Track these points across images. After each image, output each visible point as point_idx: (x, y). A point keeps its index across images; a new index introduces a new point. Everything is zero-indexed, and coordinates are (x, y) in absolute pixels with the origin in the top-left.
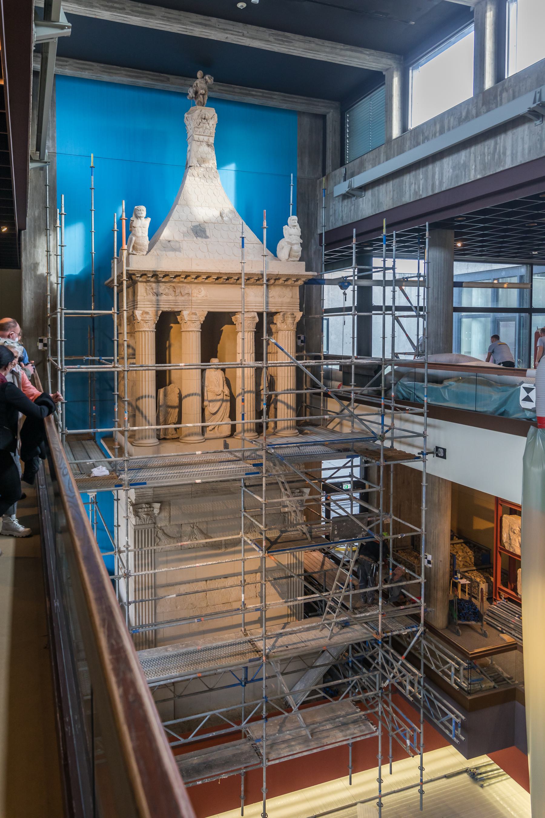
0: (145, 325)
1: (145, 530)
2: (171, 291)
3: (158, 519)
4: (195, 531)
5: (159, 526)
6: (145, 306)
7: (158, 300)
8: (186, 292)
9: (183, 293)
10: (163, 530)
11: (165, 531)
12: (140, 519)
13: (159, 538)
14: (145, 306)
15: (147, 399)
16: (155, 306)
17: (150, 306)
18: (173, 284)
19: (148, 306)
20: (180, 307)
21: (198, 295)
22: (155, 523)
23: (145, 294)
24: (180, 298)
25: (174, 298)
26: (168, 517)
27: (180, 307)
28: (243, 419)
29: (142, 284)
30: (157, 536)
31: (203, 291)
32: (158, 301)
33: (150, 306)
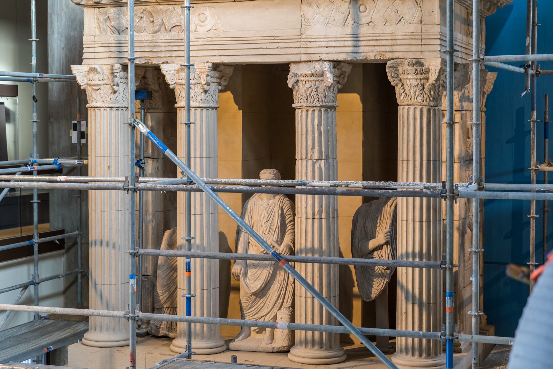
0: (94, 95)
2: (145, 23)
6: (97, 55)
7: (119, 42)
8: (174, 22)
9: (167, 24)
14: (97, 55)
15: (98, 247)
16: (115, 55)
17: (106, 55)
18: (149, 8)
19: (101, 55)
20: (162, 55)
21: (199, 29)
23: (97, 31)
24: (163, 36)
25: (150, 37)
27: (162, 55)
28: (189, 313)
29: (92, 10)
31: (209, 19)
32: (120, 44)
33: (106, 55)
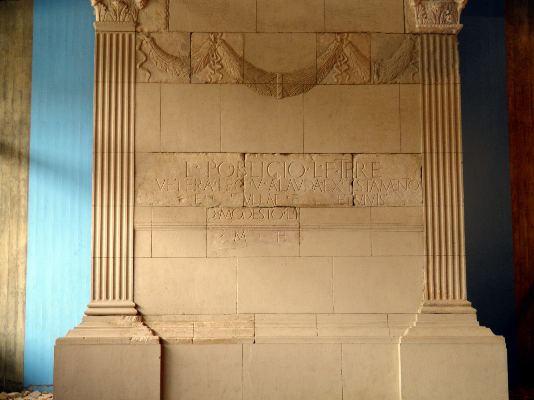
1: (118, 36)
3: (143, 16)
4: (219, 49)
5: (146, 30)
10: (153, 40)
11: (157, 42)
12: (107, 9)
13: (146, 55)
22: (137, 24)
26: (164, 16)
30: (140, 49)
